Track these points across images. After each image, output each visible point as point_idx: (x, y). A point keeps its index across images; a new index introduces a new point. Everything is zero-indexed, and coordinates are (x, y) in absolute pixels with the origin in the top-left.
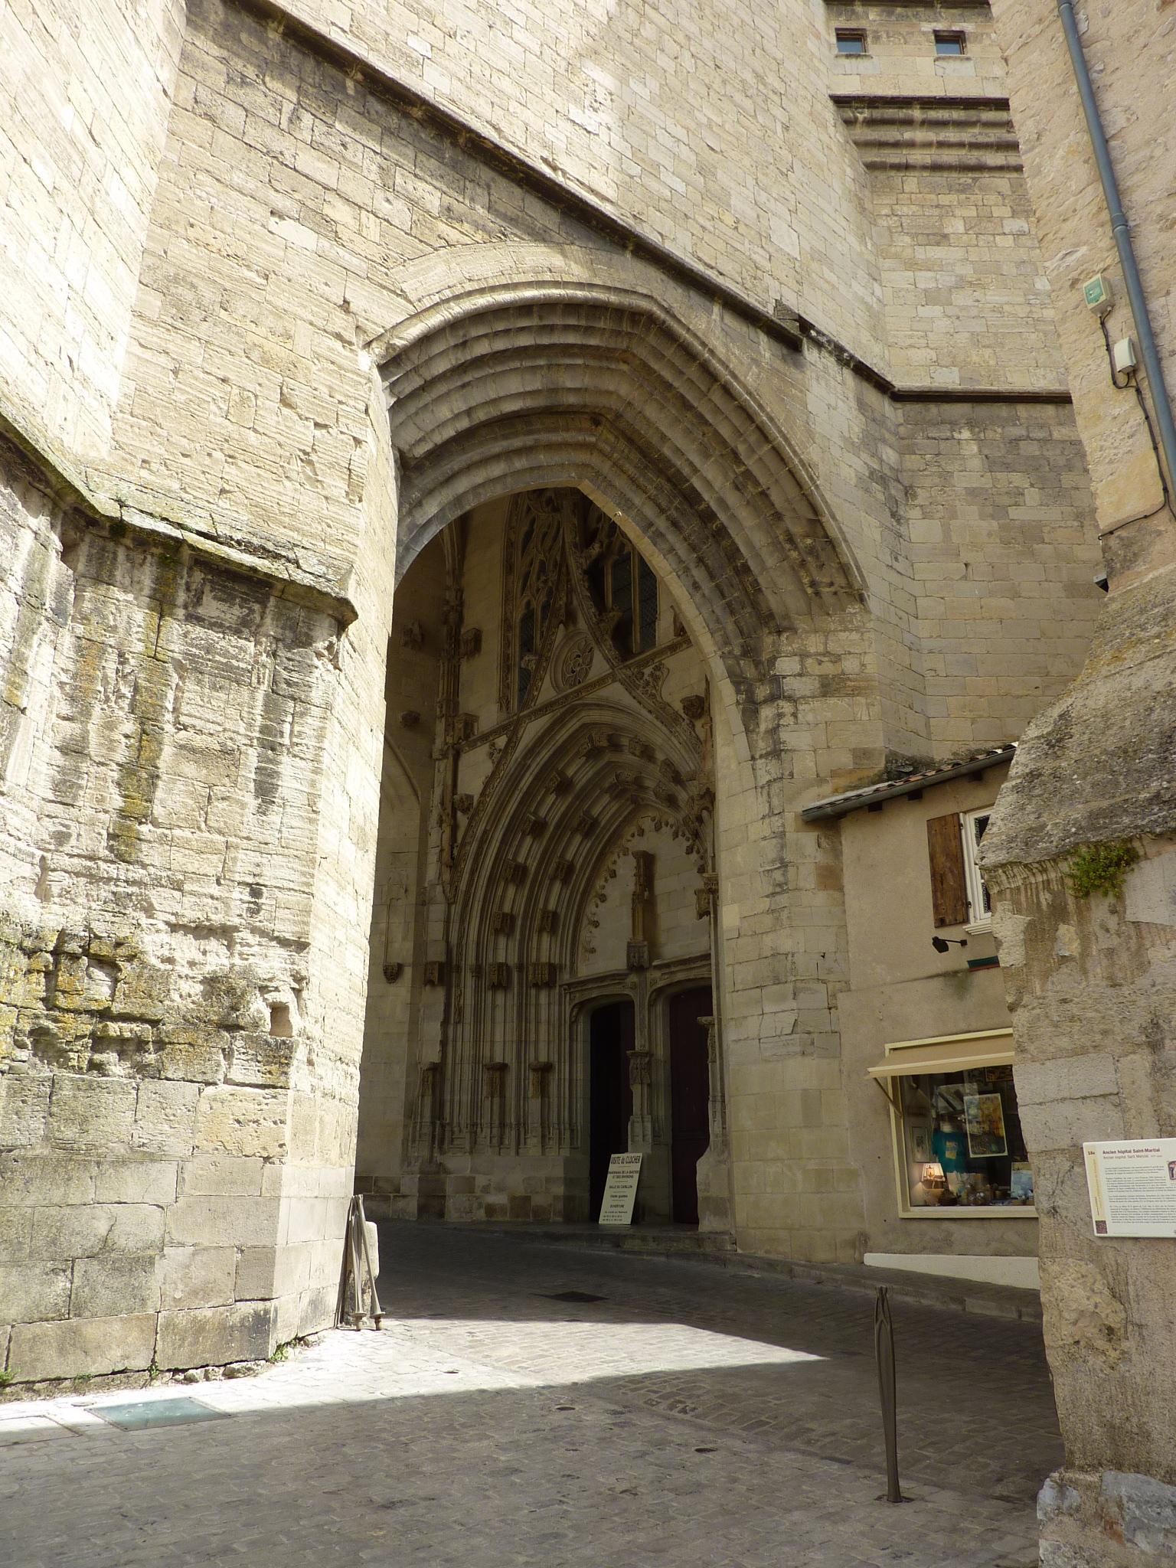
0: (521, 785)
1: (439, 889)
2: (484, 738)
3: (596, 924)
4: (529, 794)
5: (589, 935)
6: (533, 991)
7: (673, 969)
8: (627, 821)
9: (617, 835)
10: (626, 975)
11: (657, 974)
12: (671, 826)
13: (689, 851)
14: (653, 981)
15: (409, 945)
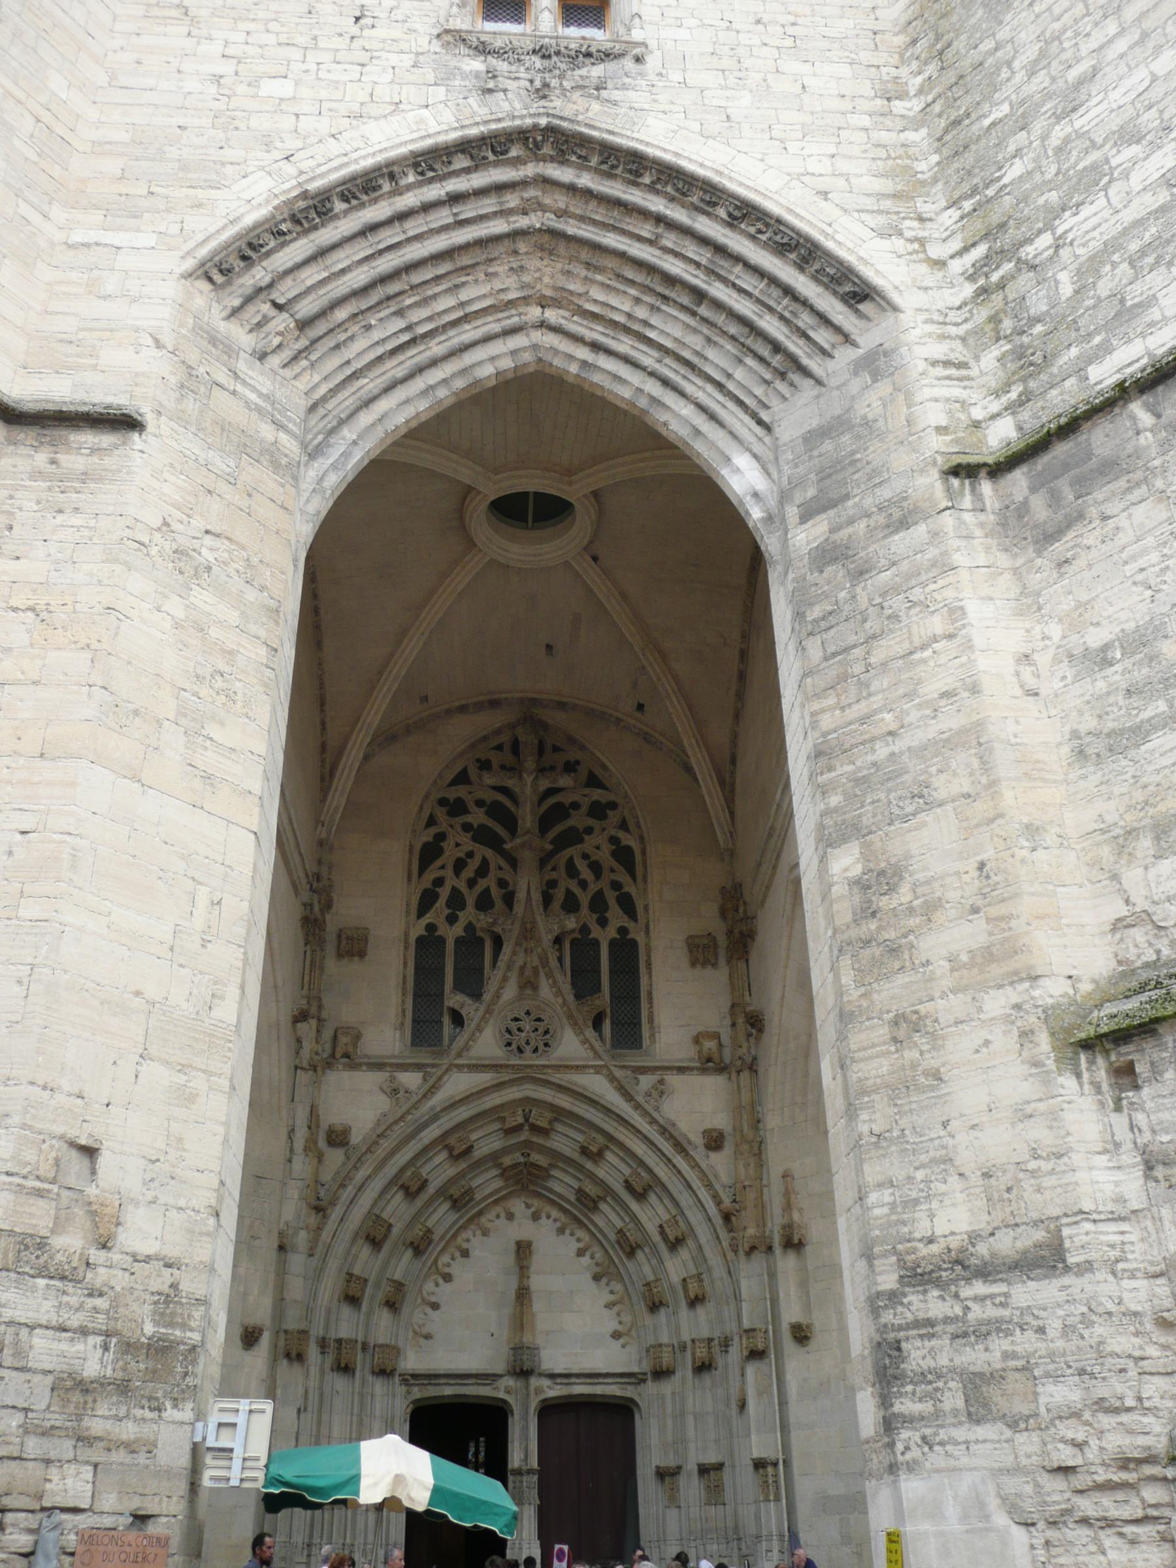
0: (423, 1134)
1: (303, 1234)
2: (379, 1066)
3: (435, 1306)
4: (426, 1149)
5: (422, 1316)
6: (369, 1377)
7: (573, 1380)
8: (496, 1202)
9: (480, 1213)
10: (501, 1376)
11: (545, 1382)
12: (555, 1220)
13: (581, 1253)
14: (538, 1391)
15: (267, 1302)
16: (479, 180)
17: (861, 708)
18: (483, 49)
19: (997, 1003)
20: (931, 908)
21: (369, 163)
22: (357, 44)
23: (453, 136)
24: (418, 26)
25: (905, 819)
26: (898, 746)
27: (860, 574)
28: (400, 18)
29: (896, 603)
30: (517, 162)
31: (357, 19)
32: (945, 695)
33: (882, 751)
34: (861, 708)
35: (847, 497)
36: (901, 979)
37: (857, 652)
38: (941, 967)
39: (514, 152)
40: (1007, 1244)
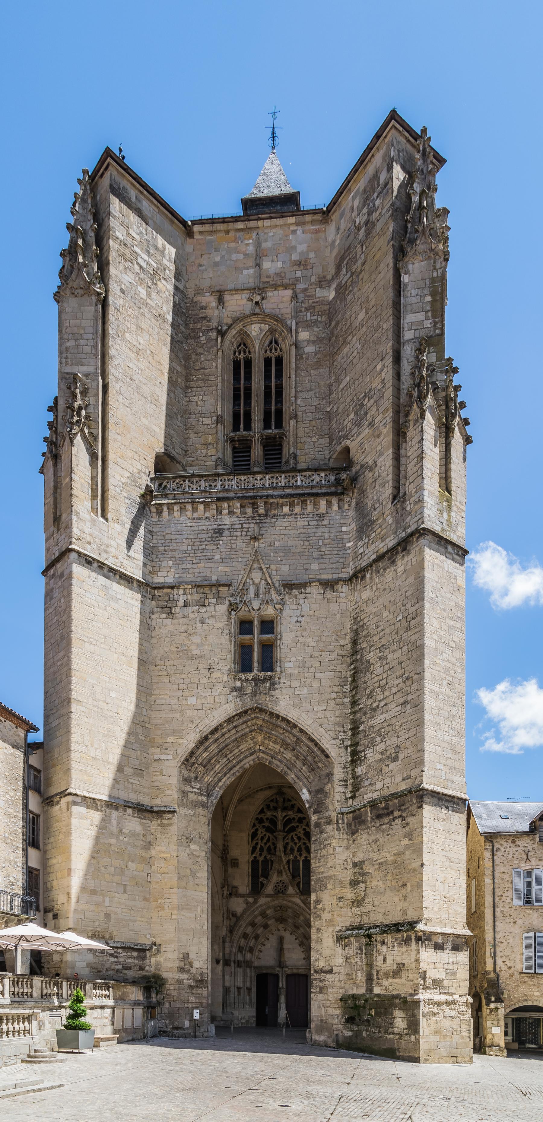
16: (241, 721)
17: (318, 865)
18: (240, 679)
19: (331, 929)
20: (324, 909)
21: (215, 726)
22: (209, 681)
23: (234, 714)
24: (224, 671)
25: (323, 891)
26: (323, 875)
27: (322, 832)
28: (219, 668)
29: (326, 842)
30: (250, 715)
31: (209, 669)
32: (331, 867)
33: (321, 876)
34: (318, 865)
35: (321, 812)
36: (319, 922)
37: (319, 851)
38: (324, 921)
39: (249, 712)
40: (327, 968)
